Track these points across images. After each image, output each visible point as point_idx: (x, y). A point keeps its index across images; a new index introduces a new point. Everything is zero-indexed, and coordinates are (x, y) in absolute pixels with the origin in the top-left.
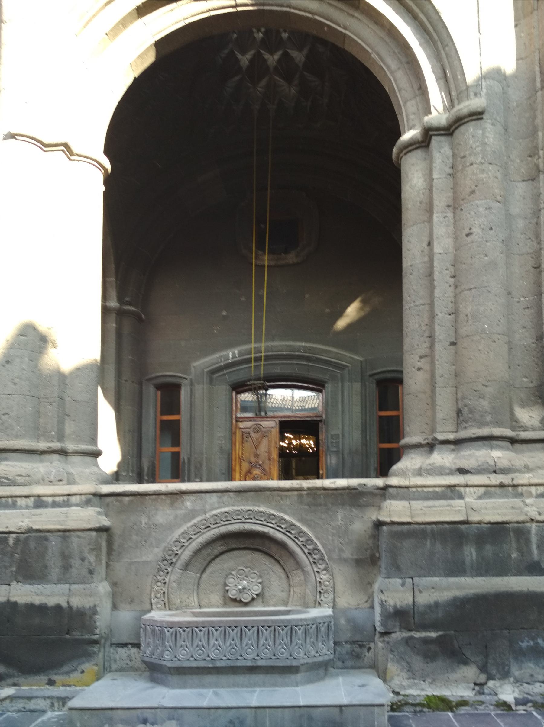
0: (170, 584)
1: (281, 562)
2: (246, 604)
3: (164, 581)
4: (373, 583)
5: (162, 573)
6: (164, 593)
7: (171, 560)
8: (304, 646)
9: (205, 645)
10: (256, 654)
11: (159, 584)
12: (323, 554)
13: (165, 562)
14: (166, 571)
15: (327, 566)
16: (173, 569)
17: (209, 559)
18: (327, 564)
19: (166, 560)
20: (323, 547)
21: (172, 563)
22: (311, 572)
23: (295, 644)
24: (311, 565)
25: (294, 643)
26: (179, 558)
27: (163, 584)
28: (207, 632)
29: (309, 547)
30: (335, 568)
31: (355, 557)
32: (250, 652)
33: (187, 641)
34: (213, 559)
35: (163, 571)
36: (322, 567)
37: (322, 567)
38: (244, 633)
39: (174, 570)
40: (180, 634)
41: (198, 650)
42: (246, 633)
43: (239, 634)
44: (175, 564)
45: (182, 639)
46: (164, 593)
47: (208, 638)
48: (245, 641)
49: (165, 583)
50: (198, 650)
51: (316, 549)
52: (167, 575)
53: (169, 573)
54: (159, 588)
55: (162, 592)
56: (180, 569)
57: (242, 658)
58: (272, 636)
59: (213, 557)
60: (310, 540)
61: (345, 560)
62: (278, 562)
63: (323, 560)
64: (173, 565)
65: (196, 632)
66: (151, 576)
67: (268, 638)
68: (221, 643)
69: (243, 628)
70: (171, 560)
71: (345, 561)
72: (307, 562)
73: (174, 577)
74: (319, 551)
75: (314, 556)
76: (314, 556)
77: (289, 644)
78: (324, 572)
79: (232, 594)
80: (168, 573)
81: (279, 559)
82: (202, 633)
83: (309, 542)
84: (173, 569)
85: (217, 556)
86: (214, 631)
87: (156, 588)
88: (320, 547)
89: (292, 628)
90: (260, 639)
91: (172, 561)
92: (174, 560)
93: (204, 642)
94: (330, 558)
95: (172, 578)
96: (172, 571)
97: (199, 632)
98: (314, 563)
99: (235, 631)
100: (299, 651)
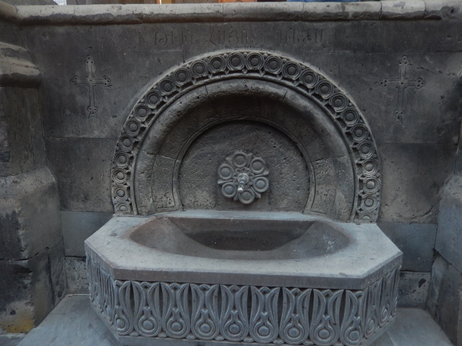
0: (137, 176)
1: (300, 145)
2: (247, 207)
3: (127, 171)
4: (443, 184)
5: (123, 158)
6: (129, 188)
7: (135, 137)
8: (363, 324)
9: (183, 314)
10: (275, 336)
11: (121, 175)
12: (369, 135)
13: (127, 141)
14: (130, 155)
15: (375, 156)
16: (139, 152)
17: (193, 137)
18: (375, 153)
19: (128, 138)
20: (370, 124)
21: (136, 143)
22: (350, 165)
23: (349, 322)
24: (350, 153)
25: (346, 322)
26: (147, 135)
27: (126, 175)
28: (186, 292)
29: (348, 123)
30: (385, 159)
31: (420, 141)
32: (263, 330)
33: (151, 304)
34: (199, 137)
35: (124, 155)
36: (368, 156)
37: (368, 156)
38: (254, 298)
39: (141, 155)
40: (140, 294)
41: (172, 323)
42: (257, 297)
43: (245, 299)
44: (142, 144)
45: (143, 302)
46: (129, 188)
47: (190, 302)
48: (257, 312)
49: (129, 174)
50: (172, 323)
51: (359, 127)
52: (132, 162)
53: (135, 159)
54: (122, 181)
55: (126, 186)
56: (151, 154)
57: (250, 340)
58: (307, 305)
59: (198, 133)
60: (351, 111)
61: (404, 147)
62: (294, 144)
63: (369, 145)
64: (138, 146)
65: (167, 291)
66: (110, 162)
67: (299, 308)
68: (213, 314)
69: (252, 288)
70: (135, 137)
71: (404, 147)
72: (344, 148)
73: (141, 165)
74: (364, 130)
75: (357, 139)
76: (357, 139)
77: (338, 322)
78: (369, 166)
79: (226, 192)
80: (132, 158)
81: (296, 140)
82: (178, 292)
83: (350, 115)
84: (139, 152)
85: (205, 132)
86: (200, 292)
87: (117, 181)
88: (367, 125)
89: (344, 293)
90: (284, 310)
91: (137, 140)
92: (140, 138)
93: (182, 308)
94: (379, 144)
95: (138, 167)
96: (138, 155)
97: (172, 291)
98: (355, 149)
99: (238, 294)
100: (356, 335)
